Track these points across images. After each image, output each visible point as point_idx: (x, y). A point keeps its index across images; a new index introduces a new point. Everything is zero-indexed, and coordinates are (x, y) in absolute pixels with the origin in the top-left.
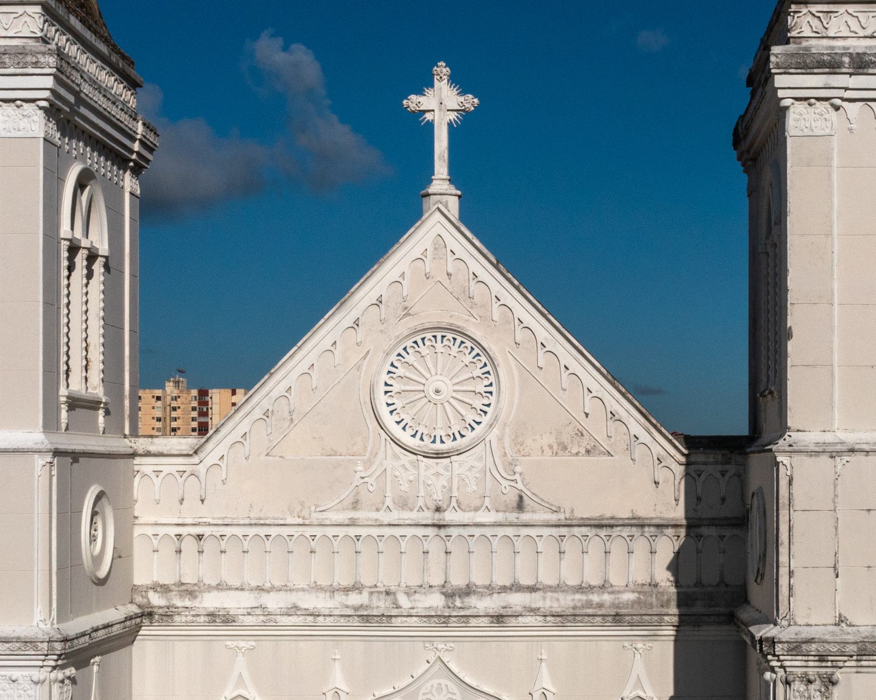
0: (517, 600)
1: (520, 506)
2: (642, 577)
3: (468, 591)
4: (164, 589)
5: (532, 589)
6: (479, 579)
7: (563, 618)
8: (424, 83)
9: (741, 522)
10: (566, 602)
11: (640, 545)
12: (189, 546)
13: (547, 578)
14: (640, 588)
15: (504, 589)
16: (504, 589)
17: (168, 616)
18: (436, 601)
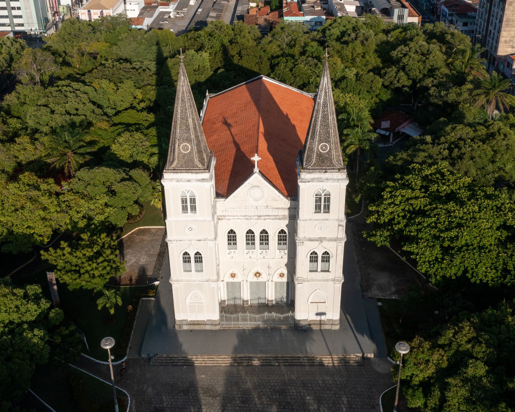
0: (267, 217)
1: (267, 206)
2: (283, 214)
3: (260, 216)
4: (221, 216)
5: (269, 216)
6: (262, 214)
7: (273, 219)
8: (253, 156)
9: (296, 208)
10: (273, 217)
11: (283, 211)
12: (224, 211)
13: (270, 214)
14: (283, 216)
15: (265, 216)
16: (265, 216)
17: (222, 219)
18: (257, 217)
